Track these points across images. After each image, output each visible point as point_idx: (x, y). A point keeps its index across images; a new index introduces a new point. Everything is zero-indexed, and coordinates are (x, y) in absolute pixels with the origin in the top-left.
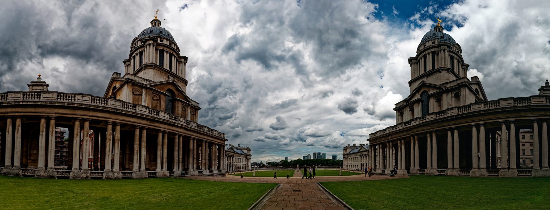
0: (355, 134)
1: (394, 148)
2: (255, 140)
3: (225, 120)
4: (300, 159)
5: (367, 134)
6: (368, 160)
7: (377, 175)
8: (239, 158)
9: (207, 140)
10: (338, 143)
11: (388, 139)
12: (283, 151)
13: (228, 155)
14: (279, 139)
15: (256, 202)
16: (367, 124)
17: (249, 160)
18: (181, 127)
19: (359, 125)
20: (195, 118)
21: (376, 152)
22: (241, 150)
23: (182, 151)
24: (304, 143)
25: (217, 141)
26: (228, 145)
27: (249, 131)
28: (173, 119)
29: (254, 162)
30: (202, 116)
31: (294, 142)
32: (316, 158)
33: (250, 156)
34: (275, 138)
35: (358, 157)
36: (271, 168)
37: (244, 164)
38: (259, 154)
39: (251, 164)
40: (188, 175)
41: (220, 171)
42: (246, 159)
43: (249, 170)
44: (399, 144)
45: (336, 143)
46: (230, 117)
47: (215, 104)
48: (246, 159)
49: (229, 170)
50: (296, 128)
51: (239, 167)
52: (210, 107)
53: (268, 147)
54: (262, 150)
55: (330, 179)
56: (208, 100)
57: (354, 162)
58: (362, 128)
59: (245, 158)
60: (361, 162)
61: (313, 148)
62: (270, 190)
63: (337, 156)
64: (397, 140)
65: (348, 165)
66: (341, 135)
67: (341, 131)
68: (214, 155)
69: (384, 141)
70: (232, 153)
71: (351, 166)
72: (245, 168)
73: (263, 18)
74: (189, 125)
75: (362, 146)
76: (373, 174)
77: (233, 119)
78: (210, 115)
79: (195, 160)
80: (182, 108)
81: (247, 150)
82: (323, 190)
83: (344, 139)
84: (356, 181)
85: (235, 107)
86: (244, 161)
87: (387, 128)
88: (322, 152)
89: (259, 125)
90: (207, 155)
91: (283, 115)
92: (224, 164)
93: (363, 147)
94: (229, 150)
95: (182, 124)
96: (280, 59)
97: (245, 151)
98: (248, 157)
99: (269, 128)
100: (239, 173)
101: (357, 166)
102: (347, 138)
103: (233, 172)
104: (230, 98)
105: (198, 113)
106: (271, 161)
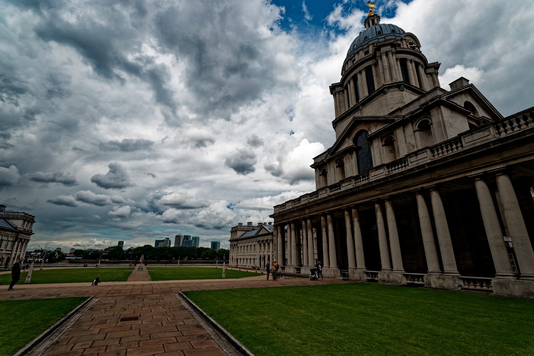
0: (251, 206)
1: (314, 229)
4: (148, 246)
5: (271, 206)
7: (287, 277)
10: (223, 221)
11: (305, 215)
12: (115, 229)
16: (269, 191)
17: (22, 244)
19: (257, 192)
29: (38, 248)
32: (181, 245)
35: (255, 245)
37: (4, 252)
38: (55, 230)
39: (28, 254)
42: (16, 240)
44: (323, 223)
45: (220, 220)
48: (14, 242)
53: (81, 218)
54: (66, 223)
55: (203, 285)
57: (248, 254)
58: (261, 197)
60: (261, 254)
61: (176, 228)
64: (319, 216)
65: (237, 259)
66: (228, 207)
67: (228, 201)
69: (298, 218)
71: (242, 260)
75: (261, 226)
76: (281, 275)
83: (232, 215)
84: (251, 289)
87: (301, 197)
88: (192, 235)
93: (263, 227)
97: (18, 224)
101: (252, 260)
102: (238, 213)
106: (83, 249)
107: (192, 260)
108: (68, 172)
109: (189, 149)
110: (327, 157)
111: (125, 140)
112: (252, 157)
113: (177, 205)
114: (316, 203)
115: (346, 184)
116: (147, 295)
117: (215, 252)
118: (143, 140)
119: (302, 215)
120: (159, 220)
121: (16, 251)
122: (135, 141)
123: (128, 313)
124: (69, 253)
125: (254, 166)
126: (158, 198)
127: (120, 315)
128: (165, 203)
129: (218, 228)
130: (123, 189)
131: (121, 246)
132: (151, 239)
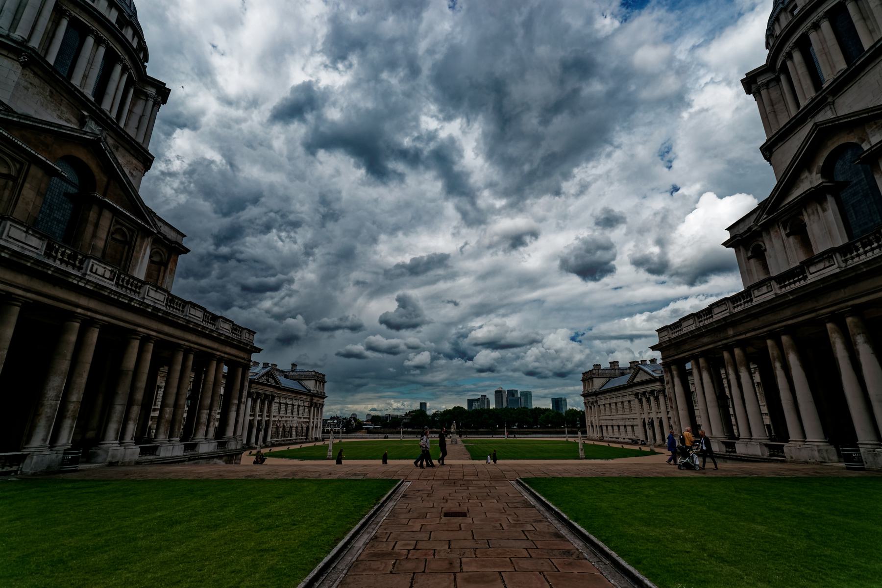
0: (613, 334)
2: (338, 354)
3: (260, 295)
4: (459, 407)
5: (651, 330)
6: (663, 407)
8: (289, 402)
9: (192, 345)
10: (567, 363)
13: (258, 393)
14: (404, 352)
15: (328, 552)
16: (645, 303)
18: (97, 293)
19: (621, 307)
20: (161, 274)
21: (690, 382)
22: (299, 380)
23: (85, 375)
24: (469, 363)
25: (228, 350)
26: (261, 365)
27: (324, 329)
28: (62, 261)
29: (334, 415)
30: (188, 273)
31: (443, 362)
33: (324, 398)
34: (392, 351)
35: (629, 402)
36: (381, 433)
37: (302, 420)
38: (348, 391)
39: (325, 421)
40: (93, 466)
41: (222, 445)
42: (311, 405)
43: (317, 440)
44: (773, 351)
45: (562, 362)
46: (276, 288)
47: (235, 247)
48: (309, 407)
49: (253, 440)
50: (450, 324)
51: (288, 431)
52: (216, 253)
53: (373, 374)
54: (357, 381)
56: (215, 231)
57: (620, 417)
58: (631, 315)
59: (307, 404)
61: (494, 379)
62: (376, 507)
63: (565, 400)
64: (764, 338)
65: (601, 427)
66: (573, 339)
67: (572, 329)
68: (210, 394)
70: (271, 389)
71: (610, 428)
72: (305, 433)
73: (374, 54)
74: (135, 292)
75: (636, 367)
77: (282, 292)
78: (215, 273)
79: (136, 410)
80: (113, 234)
81: (316, 381)
82: (538, 505)
83: (582, 351)
84: (639, 479)
85: (292, 264)
86: (304, 412)
88: (520, 389)
89: (351, 315)
90: (186, 393)
91: (416, 293)
92: (241, 420)
93: (640, 369)
94: (260, 381)
95: (98, 284)
96: (413, 158)
97: (310, 385)
98: (316, 401)
99: (379, 324)
100: (285, 448)
101: (629, 428)
102: (591, 347)
103: (267, 446)
104: (280, 238)
105: (176, 262)
106: (379, 414)
107: (525, 428)
108: (353, 315)
109: (500, 253)
110: (759, 220)
111: (413, 260)
112: (607, 247)
113: (492, 344)
114: (749, 313)
115: (821, 266)
116: (472, 480)
117: (560, 415)
118: (435, 254)
119: (720, 341)
120: (470, 369)
121: (313, 419)
122: (425, 259)
123: (451, 506)
124: (365, 420)
125: (613, 263)
126: (464, 336)
127: (442, 508)
128: (474, 342)
129: (561, 375)
130: (418, 329)
131: (423, 409)
132: (461, 397)
